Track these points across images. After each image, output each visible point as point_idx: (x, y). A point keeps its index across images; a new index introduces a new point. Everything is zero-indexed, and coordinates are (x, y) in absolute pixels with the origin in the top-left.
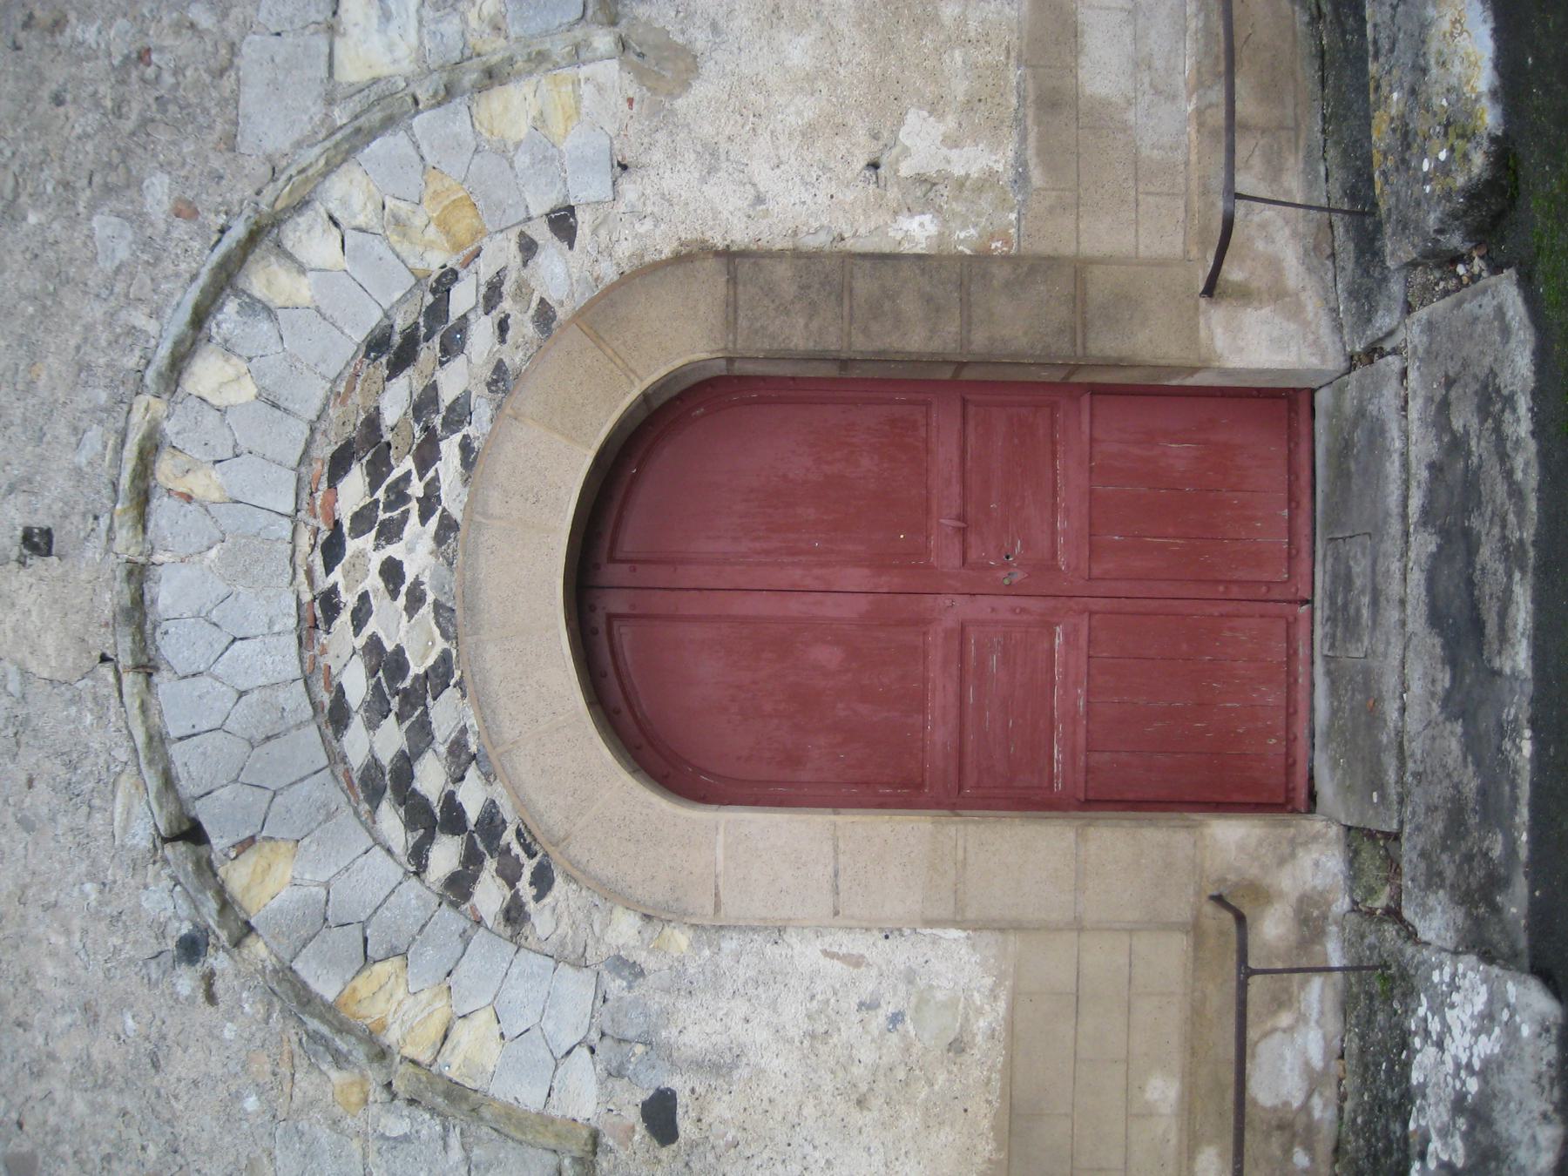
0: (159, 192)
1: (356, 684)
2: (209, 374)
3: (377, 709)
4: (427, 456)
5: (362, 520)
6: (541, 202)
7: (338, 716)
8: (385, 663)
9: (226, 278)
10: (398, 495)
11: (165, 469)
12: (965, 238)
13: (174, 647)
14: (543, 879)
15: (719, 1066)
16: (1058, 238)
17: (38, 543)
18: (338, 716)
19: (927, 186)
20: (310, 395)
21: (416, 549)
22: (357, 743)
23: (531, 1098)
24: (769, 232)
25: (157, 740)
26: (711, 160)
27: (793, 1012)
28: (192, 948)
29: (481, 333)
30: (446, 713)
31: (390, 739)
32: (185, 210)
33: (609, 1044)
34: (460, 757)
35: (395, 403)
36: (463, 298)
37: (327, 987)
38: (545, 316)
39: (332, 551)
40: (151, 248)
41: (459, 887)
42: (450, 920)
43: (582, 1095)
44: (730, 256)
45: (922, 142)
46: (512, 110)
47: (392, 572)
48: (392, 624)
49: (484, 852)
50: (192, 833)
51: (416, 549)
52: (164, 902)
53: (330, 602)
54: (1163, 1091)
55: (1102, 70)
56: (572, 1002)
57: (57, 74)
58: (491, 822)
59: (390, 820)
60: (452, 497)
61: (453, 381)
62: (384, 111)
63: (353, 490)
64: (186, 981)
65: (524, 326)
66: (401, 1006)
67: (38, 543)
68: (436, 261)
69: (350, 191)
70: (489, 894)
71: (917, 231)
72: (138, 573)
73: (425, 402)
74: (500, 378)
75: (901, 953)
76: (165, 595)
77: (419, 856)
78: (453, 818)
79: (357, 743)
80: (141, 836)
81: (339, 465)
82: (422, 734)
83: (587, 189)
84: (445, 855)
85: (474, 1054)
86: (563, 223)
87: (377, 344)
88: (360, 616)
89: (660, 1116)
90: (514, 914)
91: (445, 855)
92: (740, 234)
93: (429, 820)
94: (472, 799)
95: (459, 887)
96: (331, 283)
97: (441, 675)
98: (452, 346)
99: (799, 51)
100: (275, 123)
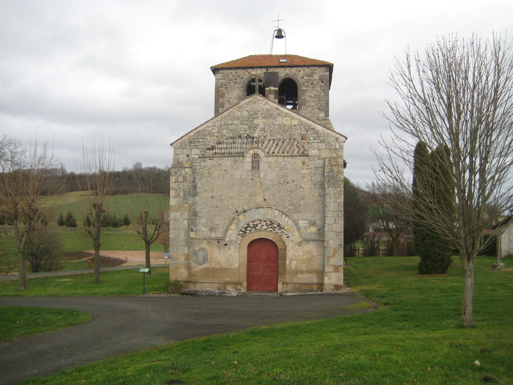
0: (290, 207)
1: (255, 223)
2: (277, 212)
3: (254, 225)
4: (271, 228)
5: (267, 223)
6: (289, 235)
7: (253, 222)
8: (257, 225)
9: (284, 213)
10: (268, 226)
11: (270, 209)
12: (287, 266)
13: (258, 210)
14: (242, 236)
15: (229, 249)
16: (287, 272)
17: (265, 200)
18: (253, 222)
19: (290, 263)
20: (275, 219)
22: (251, 223)
23: (227, 236)
24: (287, 252)
25: (251, 209)
26: (293, 248)
27: (233, 254)
28: (237, 212)
29: (280, 231)
30: (253, 230)
31: (252, 226)
32: (289, 210)
33: (231, 241)
34: (250, 230)
35: (275, 225)
36: (283, 230)
37: (234, 221)
38: (281, 236)
39: (265, 221)
40: (286, 207)
41: (241, 231)
42: (239, 230)
43: (227, 239)
44: (285, 249)
45: (294, 263)
46: (296, 233)
47: (263, 225)
48: (259, 225)
49: (244, 232)
50: (245, 212)
51: (265, 227)
52: (240, 210)
53: (261, 221)
54: (228, 279)
55: (300, 276)
56: (234, 239)
57: (299, 200)
58: (246, 233)
59: (246, 226)
60: (268, 230)
62: (296, 224)
64: (234, 211)
65: (281, 234)
66: (233, 227)
67: (265, 200)
68: (285, 228)
69: (290, 222)
70: (241, 233)
71: (287, 262)
72: (263, 207)
73: (275, 227)
74: (277, 233)
75: (237, 261)
76: (261, 209)
77: (243, 228)
78: (246, 230)
79: (251, 223)
80: (244, 208)
81: (271, 221)
82: (252, 228)
83: (290, 239)
84: (244, 230)
85: (230, 232)
86: (288, 237)
87: (279, 224)
88: (260, 223)
89: (226, 245)
90: (240, 234)
91: (244, 230)
92: (287, 250)
93: (246, 228)
94: (247, 231)
95: (241, 231)
96: (284, 221)
97: (256, 229)
98: (279, 229)
99: (301, 254)
100: (295, 216)
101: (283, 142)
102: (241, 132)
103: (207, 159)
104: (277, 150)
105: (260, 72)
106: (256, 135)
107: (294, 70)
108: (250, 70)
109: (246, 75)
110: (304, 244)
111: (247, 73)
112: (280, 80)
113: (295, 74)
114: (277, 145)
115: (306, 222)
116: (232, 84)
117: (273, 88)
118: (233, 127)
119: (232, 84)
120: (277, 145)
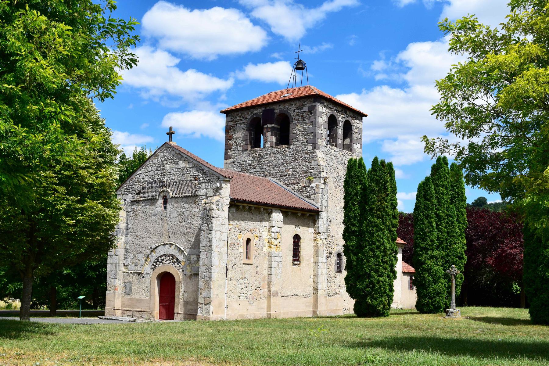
1: (162, 258)
8: (163, 260)
21: (168, 262)
30: (161, 264)
31: (160, 260)
41: (153, 265)
48: (165, 260)
49: (154, 267)
61: (176, 264)
63: (171, 257)
70: (153, 267)
82: (160, 262)
84: (155, 264)
91: (155, 264)
93: (156, 263)
94: (157, 266)
95: (153, 265)
101: (182, 184)
102: (156, 178)
103: (135, 203)
104: (178, 192)
105: (259, 111)
106: (165, 179)
107: (287, 106)
108: (252, 110)
109: (249, 116)
110: (193, 277)
111: (250, 113)
112: (276, 116)
113: (287, 109)
114: (178, 187)
115: (195, 256)
116: (238, 125)
117: (269, 126)
118: (151, 173)
119: (238, 125)
120: (178, 187)
